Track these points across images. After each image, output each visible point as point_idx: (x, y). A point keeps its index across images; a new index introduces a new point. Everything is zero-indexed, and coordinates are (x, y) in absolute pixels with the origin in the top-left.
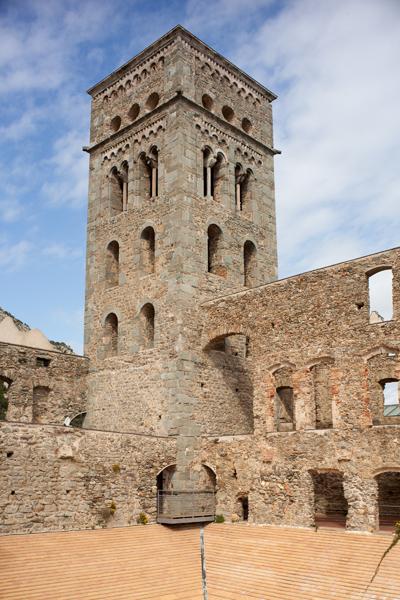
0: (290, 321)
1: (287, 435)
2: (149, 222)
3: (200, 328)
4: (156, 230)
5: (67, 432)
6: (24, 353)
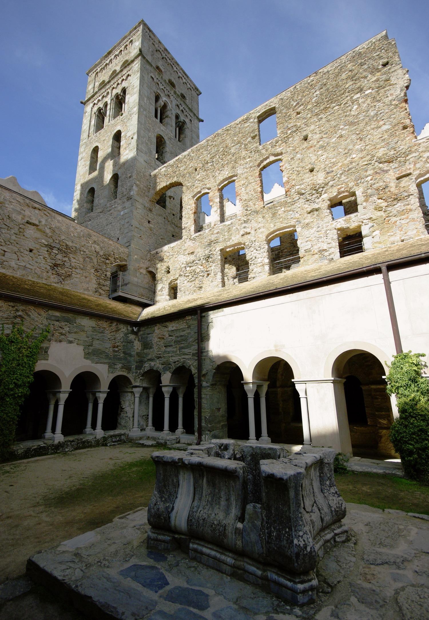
0: (207, 163)
5: (35, 208)
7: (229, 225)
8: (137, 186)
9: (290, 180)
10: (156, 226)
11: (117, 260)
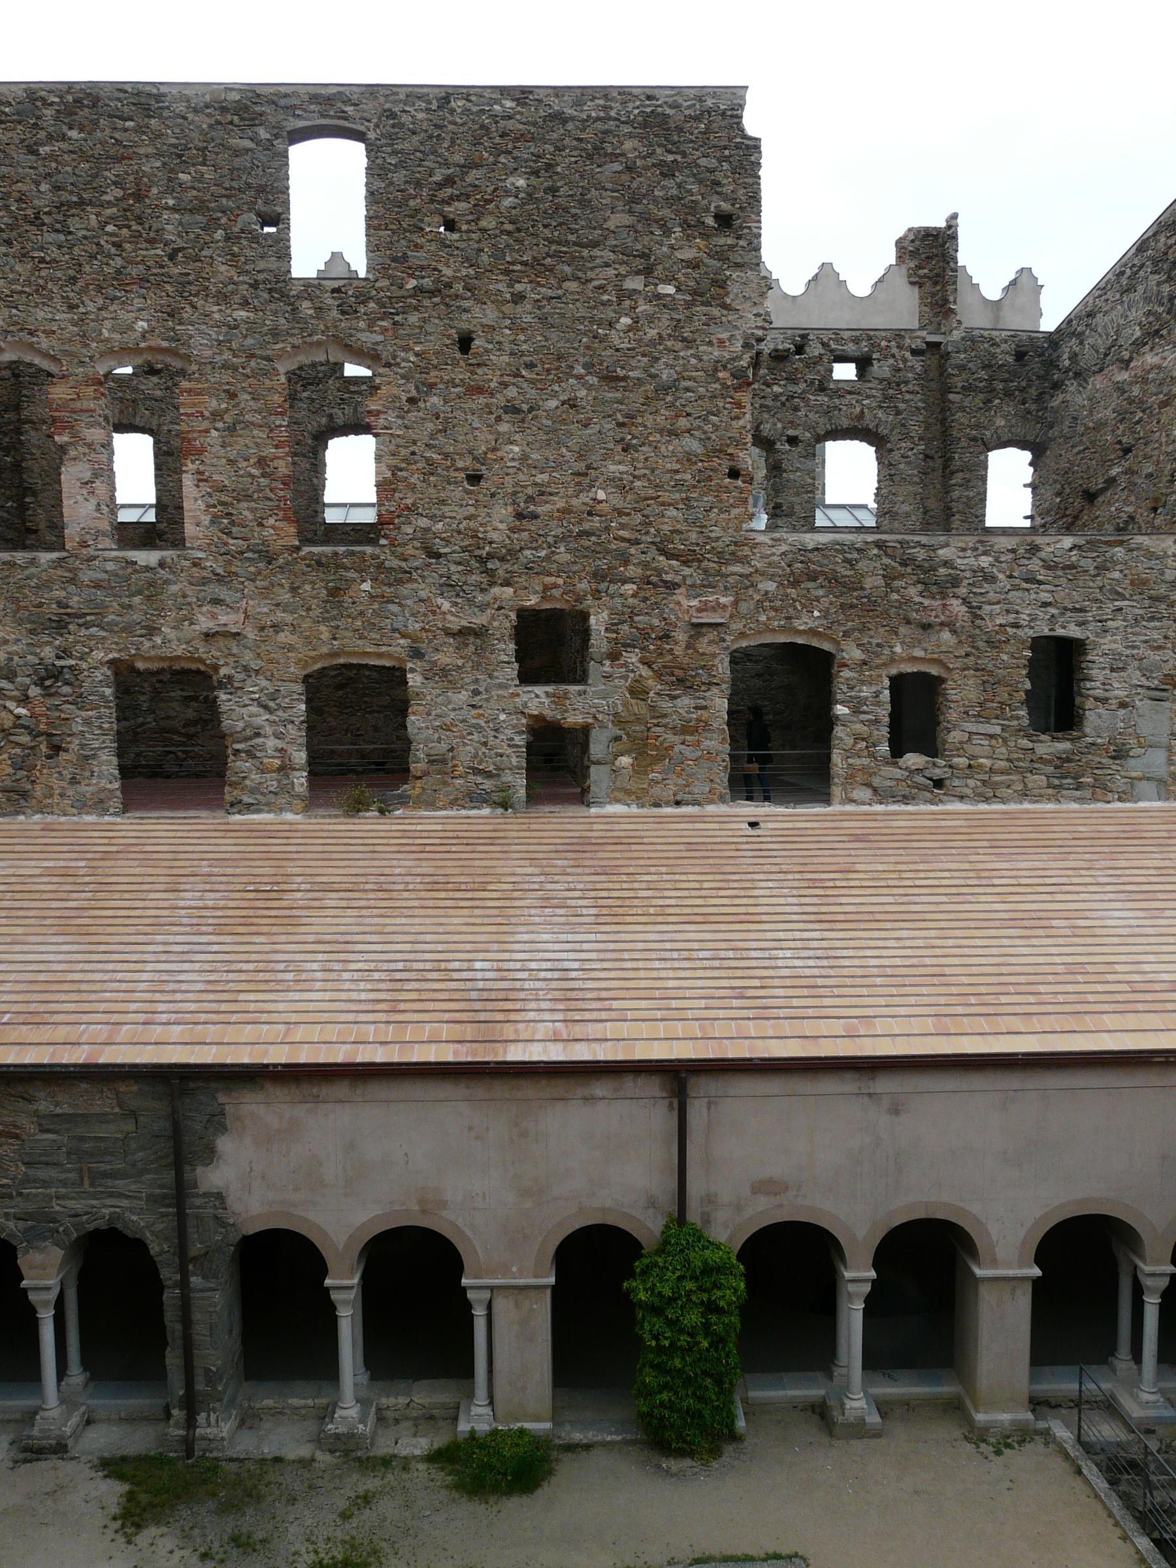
1: (33, 562)
7: (148, 569)
9: (401, 485)
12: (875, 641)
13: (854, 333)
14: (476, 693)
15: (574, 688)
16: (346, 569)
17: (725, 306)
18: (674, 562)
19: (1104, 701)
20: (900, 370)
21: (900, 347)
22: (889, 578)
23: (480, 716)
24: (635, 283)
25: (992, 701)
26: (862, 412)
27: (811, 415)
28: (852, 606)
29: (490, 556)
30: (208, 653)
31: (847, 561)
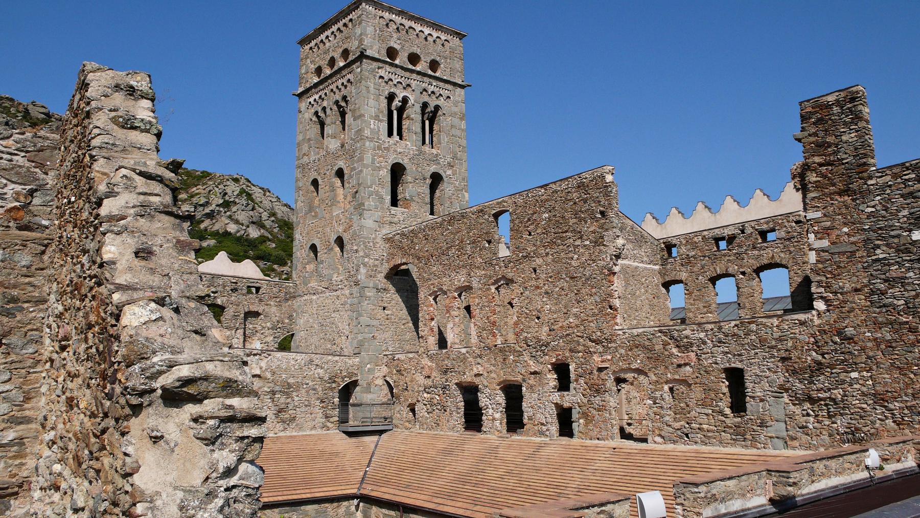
2: (341, 164)
3: (382, 257)
4: (346, 171)
6: (236, 283)
7: (464, 354)
8: (365, 265)
10: (394, 310)
11: (345, 379)
12: (660, 372)
13: (766, 220)
14: (539, 394)
15: (566, 393)
16: (507, 352)
17: (604, 245)
18: (594, 344)
19: (753, 397)
20: (789, 232)
21: (788, 222)
22: (665, 344)
23: (541, 403)
24: (578, 242)
25: (707, 398)
26: (773, 256)
27: (750, 261)
28: (651, 358)
29: (542, 345)
30: (477, 381)
31: (648, 339)
